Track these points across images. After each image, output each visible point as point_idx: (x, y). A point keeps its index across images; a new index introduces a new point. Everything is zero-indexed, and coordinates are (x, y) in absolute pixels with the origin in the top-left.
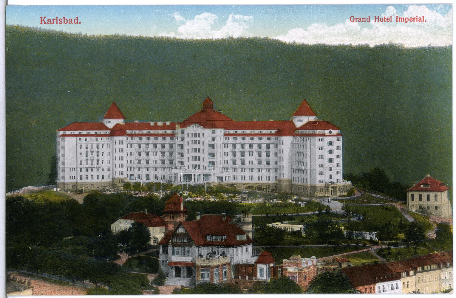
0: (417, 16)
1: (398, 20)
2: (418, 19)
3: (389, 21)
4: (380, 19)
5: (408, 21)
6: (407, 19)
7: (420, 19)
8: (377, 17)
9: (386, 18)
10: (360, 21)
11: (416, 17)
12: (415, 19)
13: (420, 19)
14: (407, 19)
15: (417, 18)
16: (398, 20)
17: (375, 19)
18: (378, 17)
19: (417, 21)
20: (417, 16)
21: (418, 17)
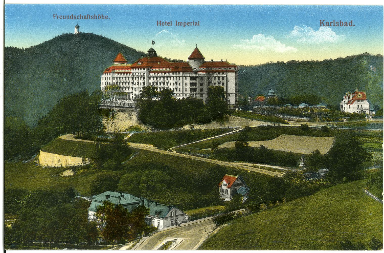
0: (193, 21)
1: (177, 24)
2: (194, 24)
3: (189, 25)
4: (162, 23)
5: (186, 25)
6: (185, 23)
7: (196, 23)
8: (159, 22)
9: (167, 22)
10: (196, 25)
11: (193, 22)
12: (192, 24)
13: (196, 23)
14: (185, 23)
15: (193, 23)
16: (177, 24)
17: (158, 23)
18: (160, 21)
19: (193, 25)
20: (193, 21)
21: (194, 22)
